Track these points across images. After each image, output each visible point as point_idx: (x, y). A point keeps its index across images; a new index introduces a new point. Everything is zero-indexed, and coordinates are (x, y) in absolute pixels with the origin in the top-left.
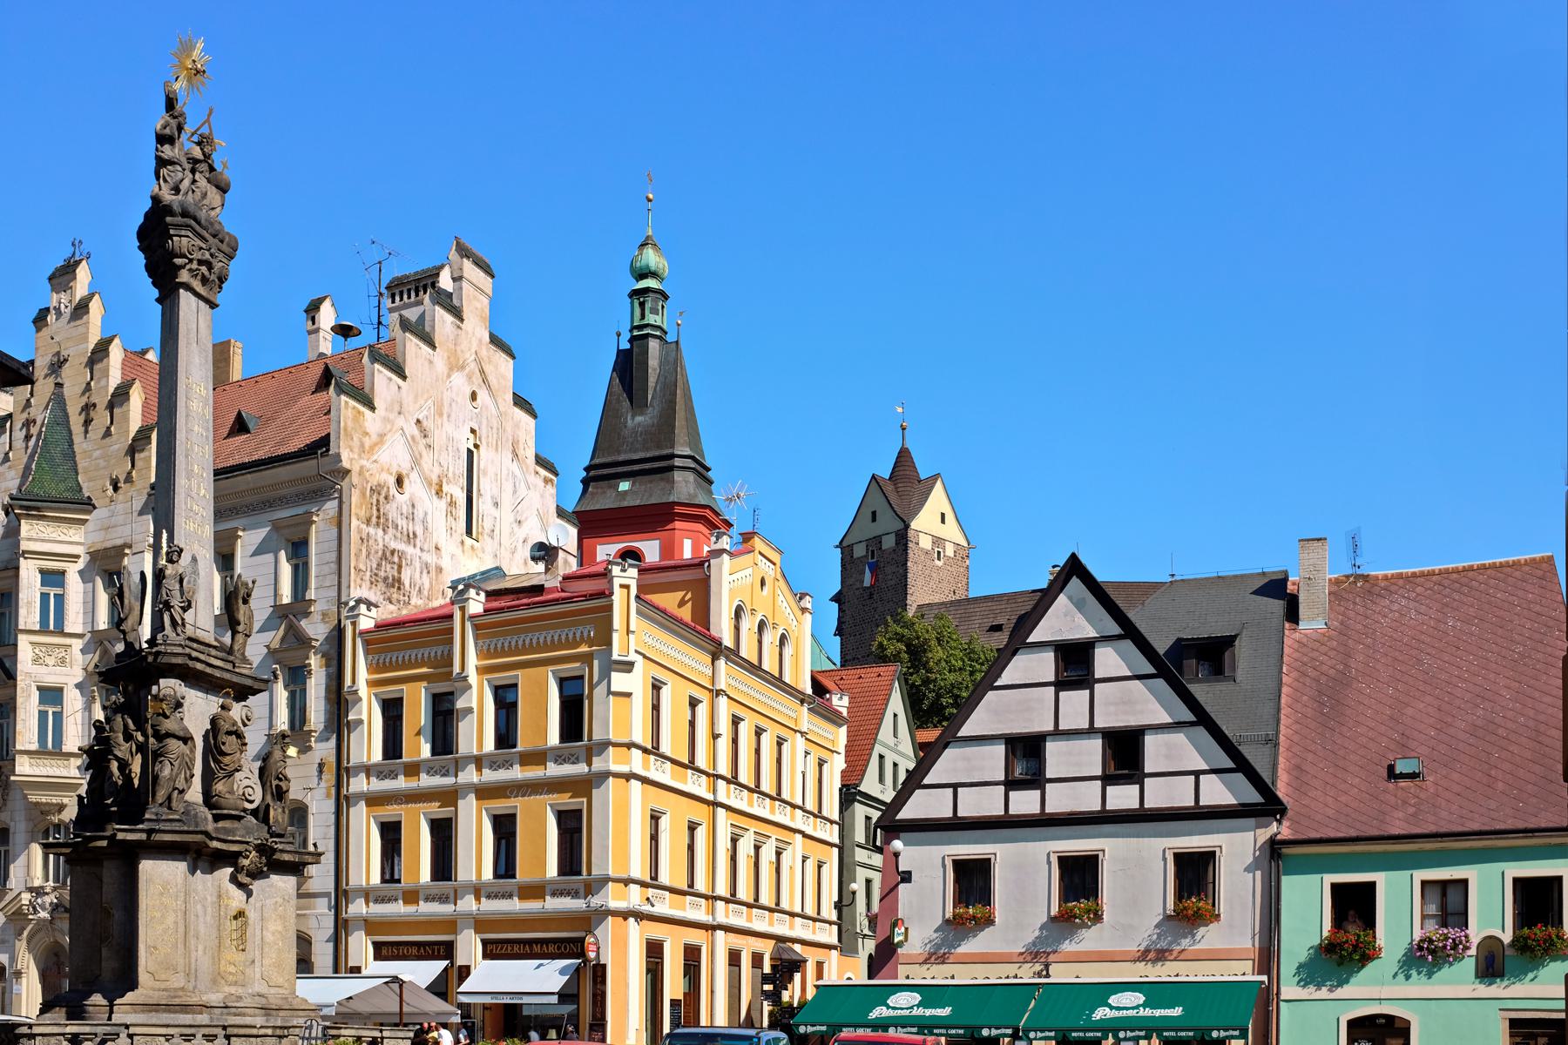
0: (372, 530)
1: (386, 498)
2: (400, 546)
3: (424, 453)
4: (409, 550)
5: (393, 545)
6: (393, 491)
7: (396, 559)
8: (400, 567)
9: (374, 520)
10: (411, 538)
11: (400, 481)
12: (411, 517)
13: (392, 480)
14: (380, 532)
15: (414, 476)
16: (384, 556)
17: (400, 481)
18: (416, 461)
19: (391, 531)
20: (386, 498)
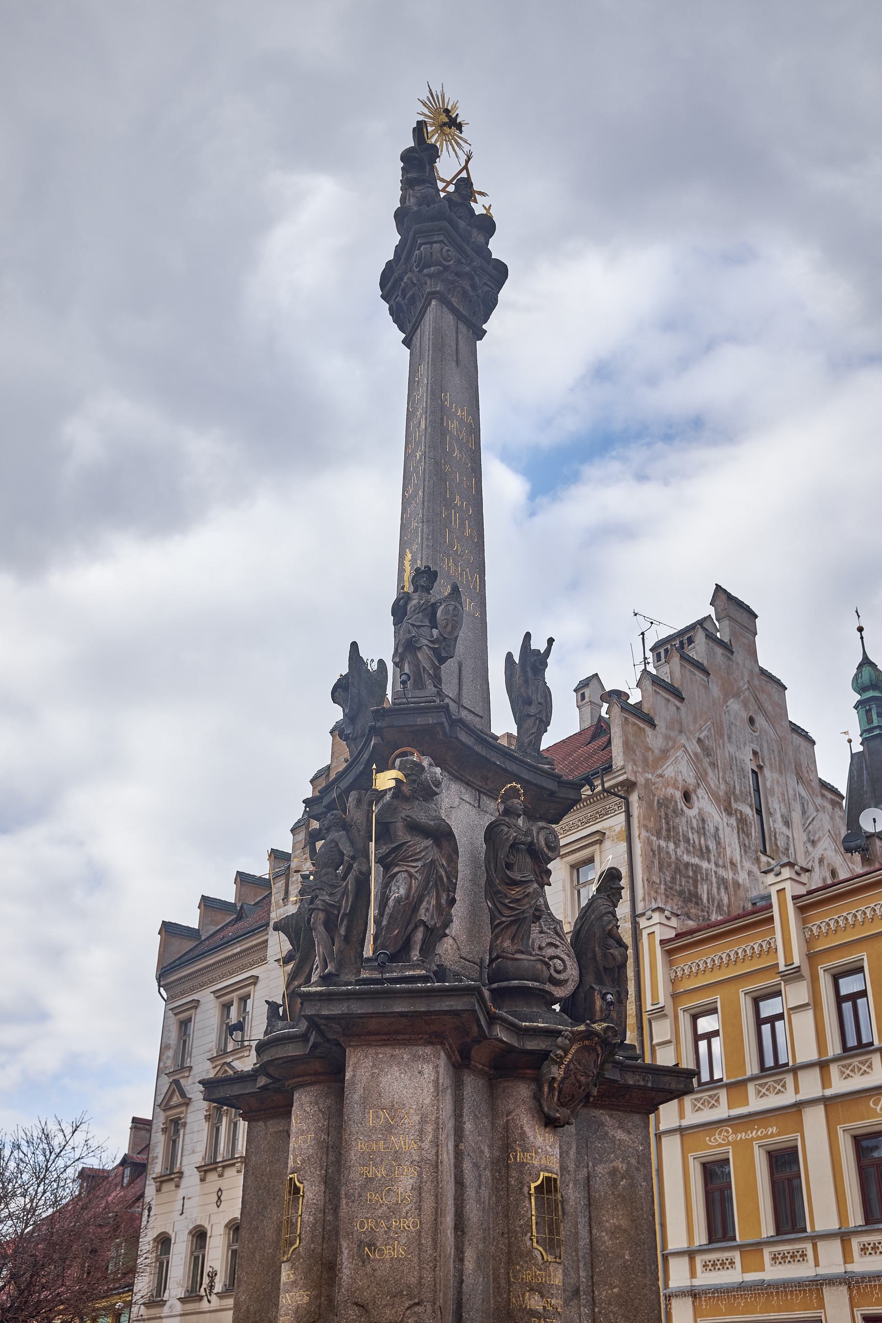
0: (663, 843)
1: (674, 811)
2: (695, 860)
3: (709, 770)
4: (705, 865)
5: (686, 858)
6: (681, 804)
7: (691, 874)
8: (696, 882)
9: (664, 833)
10: (704, 853)
11: (687, 796)
12: (702, 831)
13: (678, 795)
14: (672, 846)
15: (701, 792)
16: (677, 869)
17: (687, 796)
18: (701, 777)
19: (682, 845)
20: (674, 811)
